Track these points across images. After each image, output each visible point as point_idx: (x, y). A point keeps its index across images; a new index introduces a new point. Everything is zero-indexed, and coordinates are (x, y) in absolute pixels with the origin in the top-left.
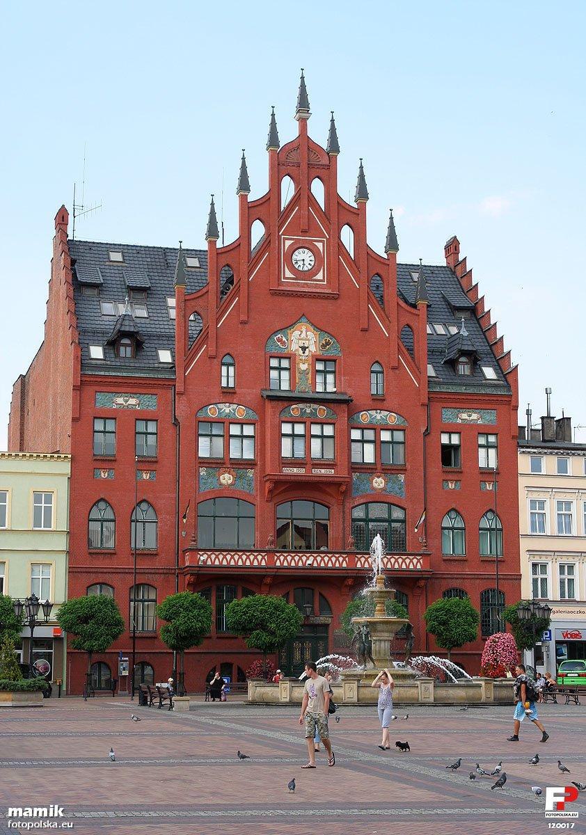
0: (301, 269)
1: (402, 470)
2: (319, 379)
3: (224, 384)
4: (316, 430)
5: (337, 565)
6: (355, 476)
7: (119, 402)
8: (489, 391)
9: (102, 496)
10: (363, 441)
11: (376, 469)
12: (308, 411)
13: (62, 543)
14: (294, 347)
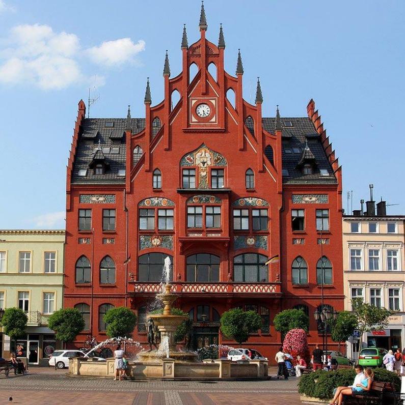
0: (202, 116)
2: (214, 181)
3: (155, 186)
4: (209, 210)
5: (221, 291)
6: (236, 238)
7: (94, 200)
8: (322, 183)
9: (83, 254)
10: (241, 217)
11: (249, 233)
13: (59, 281)
14: (198, 162)
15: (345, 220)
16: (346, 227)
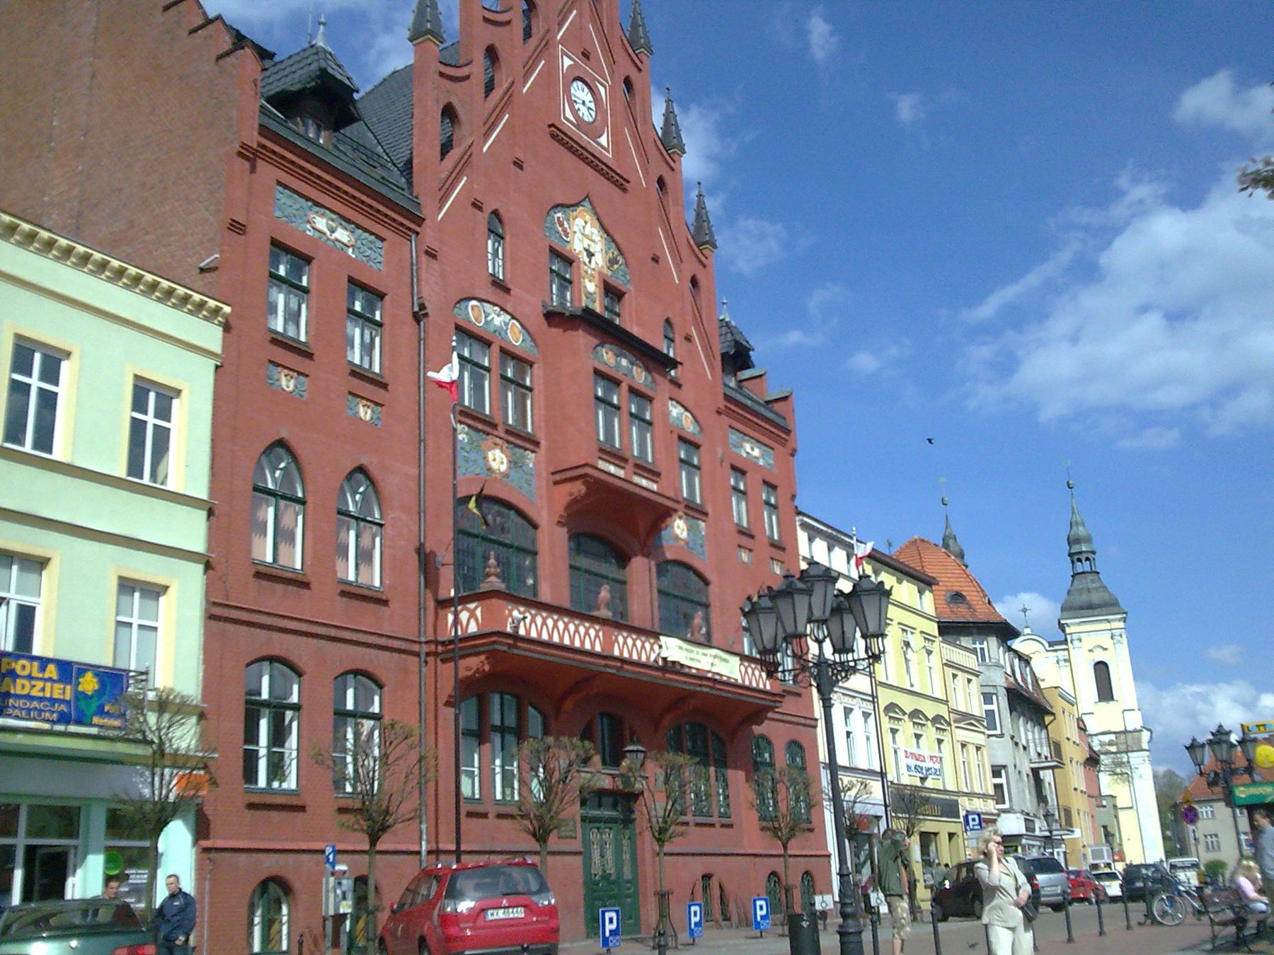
13: (191, 531)
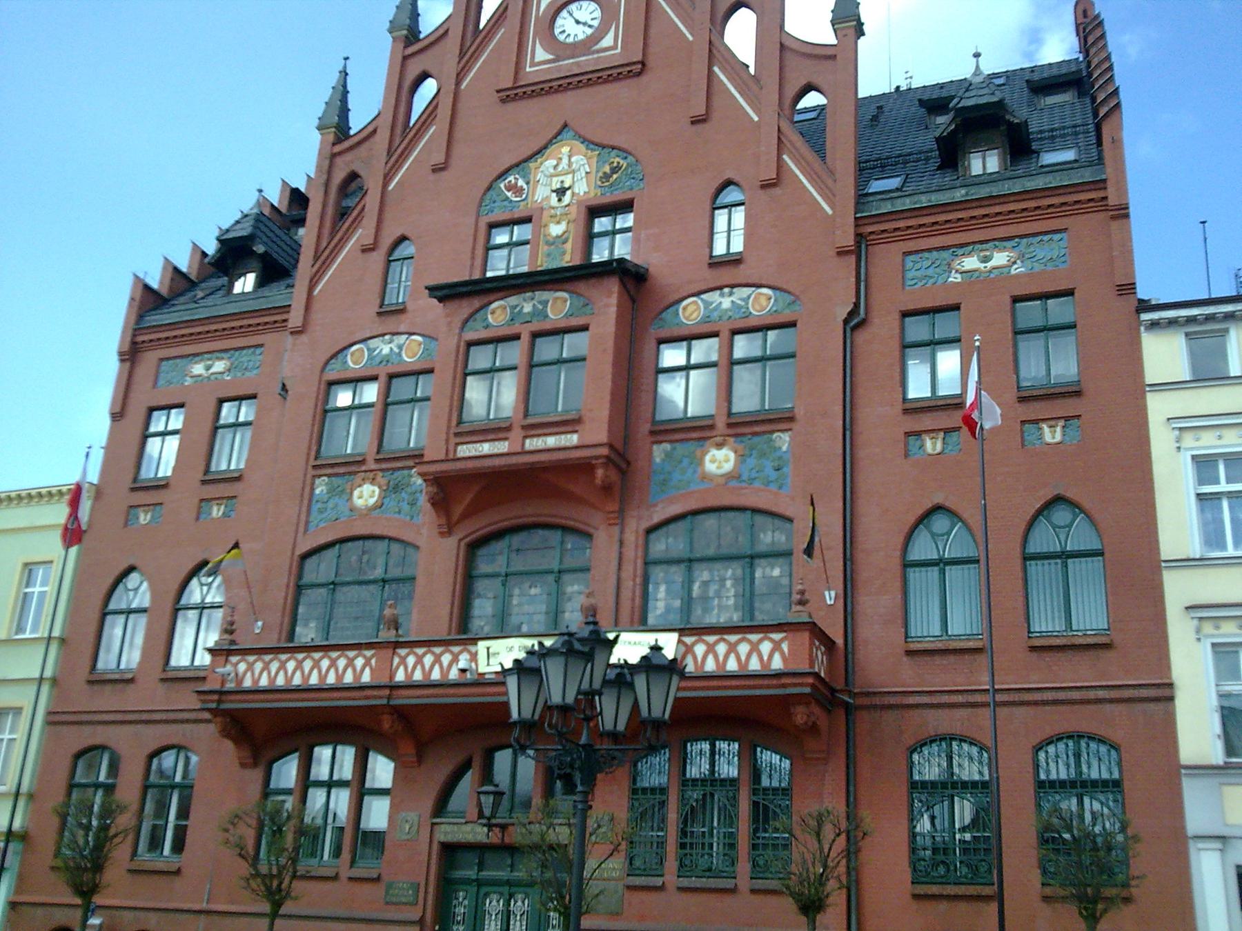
1: (784, 419)
12: (528, 308)
14: (543, 193)
15: (1154, 325)
16: (1164, 355)
